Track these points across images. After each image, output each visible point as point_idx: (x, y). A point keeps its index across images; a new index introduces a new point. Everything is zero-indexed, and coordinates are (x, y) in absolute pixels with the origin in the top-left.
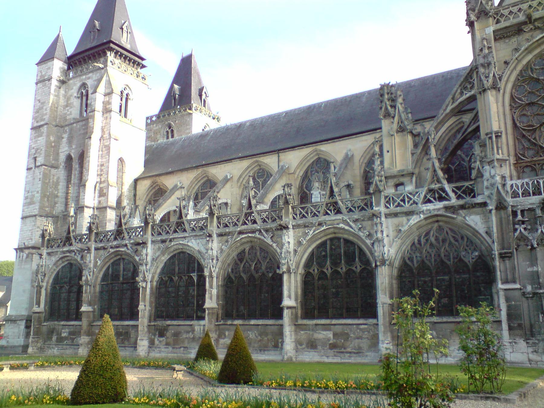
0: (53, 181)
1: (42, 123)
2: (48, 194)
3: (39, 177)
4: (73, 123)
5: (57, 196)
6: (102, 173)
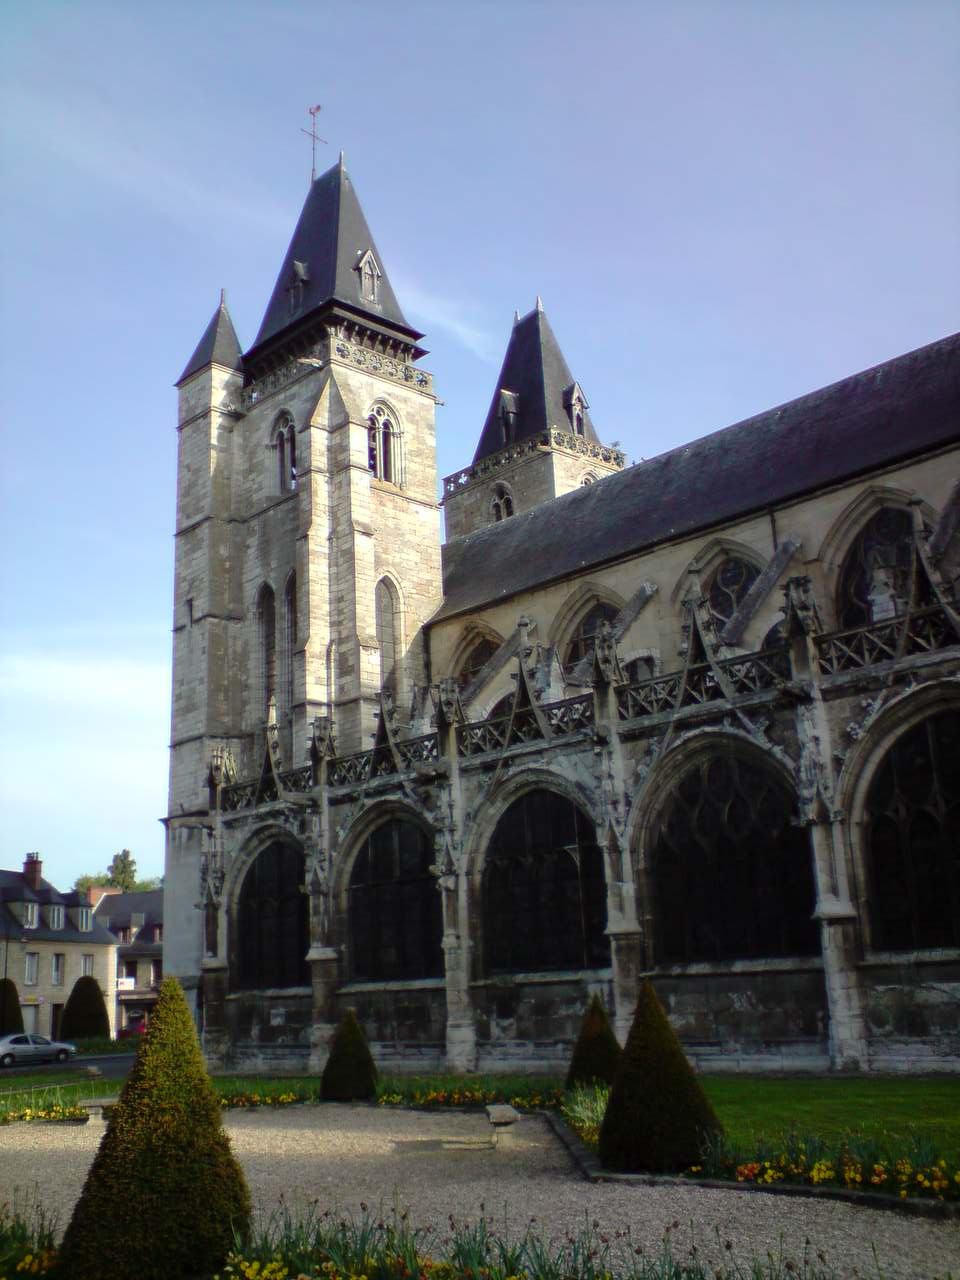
0: (235, 652)
1: (198, 518)
2: (226, 682)
4: (268, 509)
5: (247, 687)
6: (342, 617)
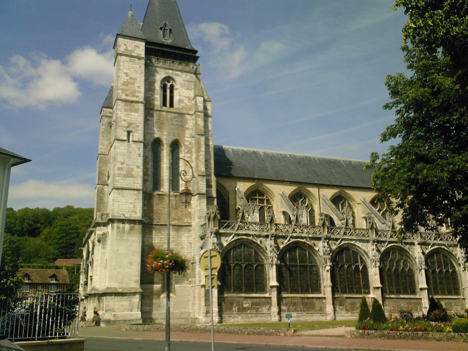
3: (137, 152)
